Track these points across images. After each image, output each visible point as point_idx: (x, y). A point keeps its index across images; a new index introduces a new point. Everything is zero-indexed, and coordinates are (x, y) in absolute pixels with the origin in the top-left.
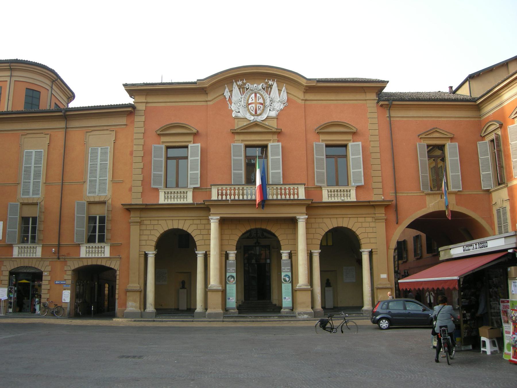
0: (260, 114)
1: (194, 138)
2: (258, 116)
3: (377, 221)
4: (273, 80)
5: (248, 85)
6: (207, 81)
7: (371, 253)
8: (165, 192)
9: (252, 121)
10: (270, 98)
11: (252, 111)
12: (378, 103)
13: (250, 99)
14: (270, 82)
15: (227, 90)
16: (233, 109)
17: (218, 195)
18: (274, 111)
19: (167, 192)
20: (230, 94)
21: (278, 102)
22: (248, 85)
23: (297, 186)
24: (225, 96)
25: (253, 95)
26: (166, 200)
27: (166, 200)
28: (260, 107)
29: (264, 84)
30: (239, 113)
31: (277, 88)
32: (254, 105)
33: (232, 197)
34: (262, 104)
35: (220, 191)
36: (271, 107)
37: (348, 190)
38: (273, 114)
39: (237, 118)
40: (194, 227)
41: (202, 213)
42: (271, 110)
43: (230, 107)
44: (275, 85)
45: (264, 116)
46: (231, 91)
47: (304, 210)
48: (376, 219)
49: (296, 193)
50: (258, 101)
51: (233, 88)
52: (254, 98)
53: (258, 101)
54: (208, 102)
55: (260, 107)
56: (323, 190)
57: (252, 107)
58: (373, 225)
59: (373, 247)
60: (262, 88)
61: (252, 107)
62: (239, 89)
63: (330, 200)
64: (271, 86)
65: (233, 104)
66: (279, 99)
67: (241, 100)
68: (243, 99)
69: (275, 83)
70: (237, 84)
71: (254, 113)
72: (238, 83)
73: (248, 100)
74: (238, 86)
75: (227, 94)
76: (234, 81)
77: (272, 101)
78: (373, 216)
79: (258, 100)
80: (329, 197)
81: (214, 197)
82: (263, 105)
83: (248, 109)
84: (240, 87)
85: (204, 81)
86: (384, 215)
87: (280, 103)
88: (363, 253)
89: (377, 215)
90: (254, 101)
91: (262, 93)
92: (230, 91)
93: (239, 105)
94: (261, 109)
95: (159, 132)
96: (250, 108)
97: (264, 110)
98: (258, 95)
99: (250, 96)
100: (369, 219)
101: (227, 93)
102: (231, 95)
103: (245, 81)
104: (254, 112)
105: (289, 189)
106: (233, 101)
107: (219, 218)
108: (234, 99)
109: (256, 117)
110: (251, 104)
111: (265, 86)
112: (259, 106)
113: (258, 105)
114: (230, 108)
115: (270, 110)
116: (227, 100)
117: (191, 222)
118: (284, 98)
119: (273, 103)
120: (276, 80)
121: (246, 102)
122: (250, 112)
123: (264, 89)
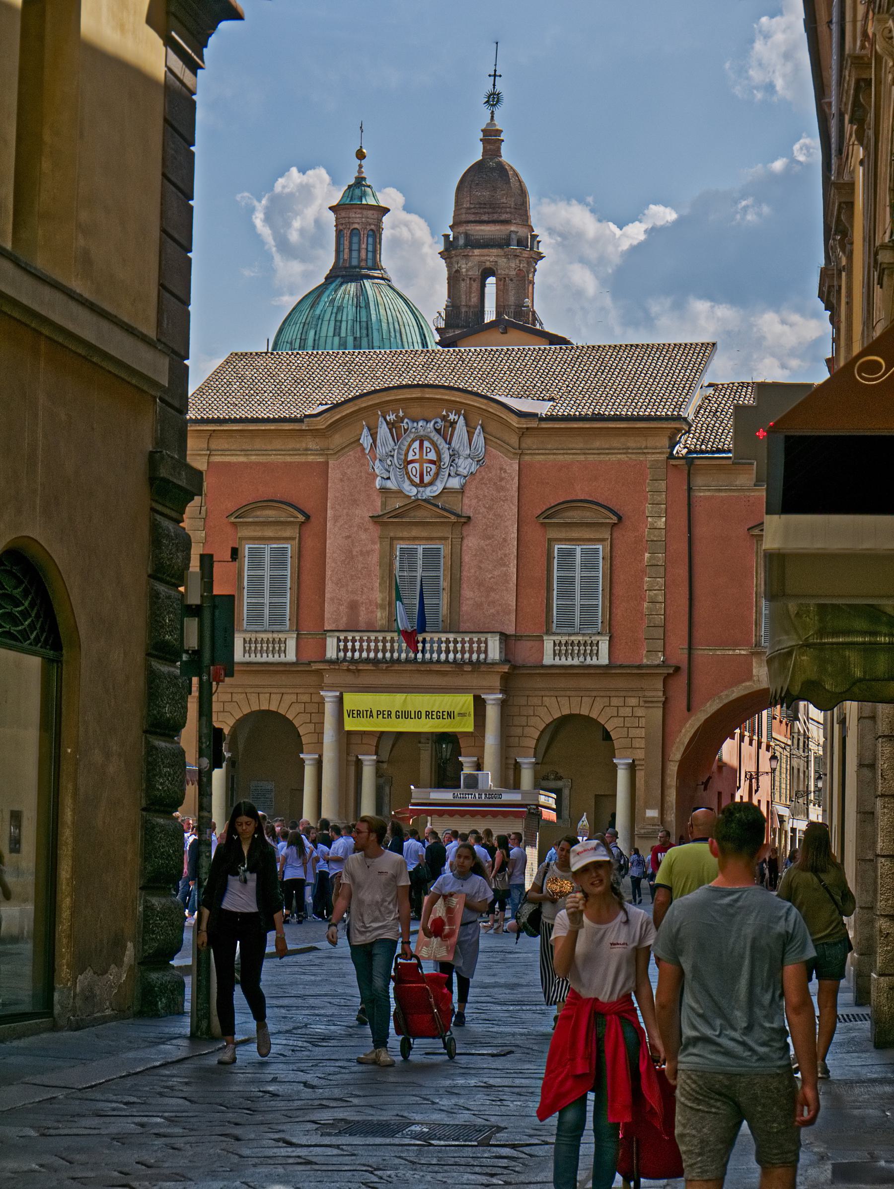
0: (431, 483)
1: (300, 529)
2: (426, 486)
3: (646, 705)
4: (458, 413)
5: (407, 423)
7: (632, 768)
8: (244, 639)
9: (413, 498)
10: (451, 451)
11: (415, 476)
12: (668, 458)
13: (411, 453)
14: (452, 417)
16: (377, 471)
17: (339, 650)
18: (458, 478)
19: (248, 640)
20: (371, 441)
21: (467, 458)
22: (407, 423)
23: (486, 635)
24: (361, 445)
25: (416, 444)
26: (247, 655)
27: (247, 655)
28: (429, 470)
29: (439, 420)
30: (389, 481)
31: (465, 428)
32: (417, 465)
33: (364, 655)
34: (432, 462)
35: (342, 644)
36: (452, 468)
37: (595, 642)
38: (455, 483)
39: (384, 490)
40: (299, 708)
41: (312, 680)
42: (452, 474)
43: (373, 468)
44: (461, 421)
45: (438, 488)
46: (374, 436)
47: (496, 682)
48: (648, 703)
49: (483, 649)
50: (425, 457)
51: (379, 429)
52: (417, 451)
53: (425, 457)
55: (429, 470)
56: (545, 642)
57: (414, 470)
58: (640, 712)
59: (640, 754)
60: (435, 428)
61: (414, 469)
62: (391, 430)
63: (557, 662)
64: (453, 424)
65: (377, 462)
66: (468, 452)
67: (392, 454)
68: (396, 451)
69: (462, 417)
70: (385, 420)
71: (417, 480)
72: (388, 418)
73: (407, 454)
74: (388, 423)
75: (366, 440)
76: (380, 413)
77: (454, 456)
78: (640, 694)
80: (555, 655)
81: (331, 653)
82: (435, 464)
83: (407, 473)
84: (391, 425)
85: (319, 418)
86: (661, 694)
87: (469, 459)
88: (619, 767)
89: (647, 694)
90: (417, 457)
91: (435, 439)
92: (371, 435)
93: (390, 463)
94: (432, 473)
95: (232, 519)
96: (410, 470)
97: (437, 474)
98: (426, 444)
99: (410, 446)
100: (633, 701)
102: (374, 441)
103: (401, 414)
104: (418, 479)
105: (471, 642)
106: (378, 456)
108: (381, 451)
109: (421, 489)
110: (412, 462)
111: (441, 424)
113: (425, 465)
114: (371, 470)
115: (449, 475)
116: (367, 452)
117: (293, 698)
118: (478, 451)
119: (457, 460)
120: (463, 412)
121: (403, 457)
122: (409, 478)
123: (438, 431)
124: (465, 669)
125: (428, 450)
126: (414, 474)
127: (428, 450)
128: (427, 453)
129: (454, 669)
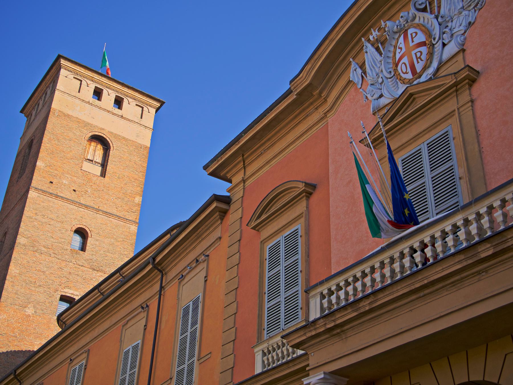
2: (420, 77)
6: (304, 73)
11: (406, 73)
15: (353, 65)
30: (383, 98)
54: (328, 116)
55: (418, 54)
60: (419, 10)
70: (369, 40)
72: (371, 38)
79: (413, 41)
95: (253, 224)
97: (431, 55)
101: (355, 72)
107: (322, 376)
112: (416, 54)
124: (483, 255)
125: (414, 35)
126: (404, 71)
127: (414, 35)
128: (412, 38)
129: (465, 264)
